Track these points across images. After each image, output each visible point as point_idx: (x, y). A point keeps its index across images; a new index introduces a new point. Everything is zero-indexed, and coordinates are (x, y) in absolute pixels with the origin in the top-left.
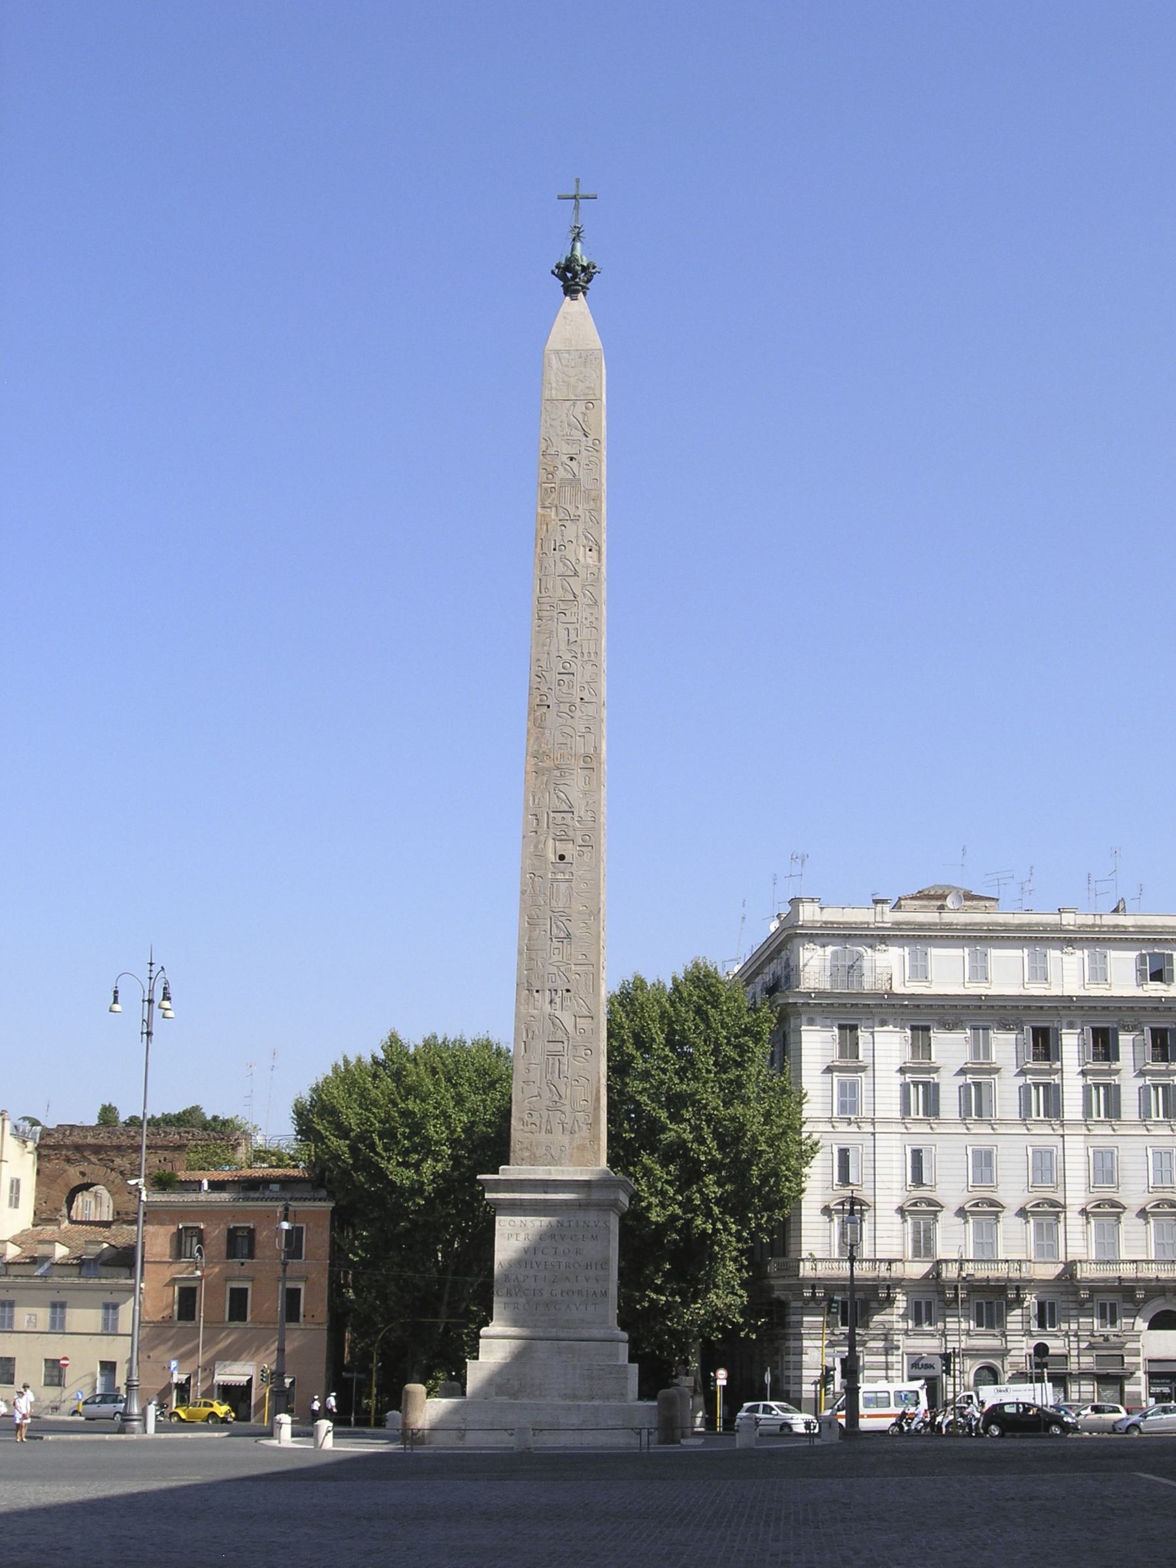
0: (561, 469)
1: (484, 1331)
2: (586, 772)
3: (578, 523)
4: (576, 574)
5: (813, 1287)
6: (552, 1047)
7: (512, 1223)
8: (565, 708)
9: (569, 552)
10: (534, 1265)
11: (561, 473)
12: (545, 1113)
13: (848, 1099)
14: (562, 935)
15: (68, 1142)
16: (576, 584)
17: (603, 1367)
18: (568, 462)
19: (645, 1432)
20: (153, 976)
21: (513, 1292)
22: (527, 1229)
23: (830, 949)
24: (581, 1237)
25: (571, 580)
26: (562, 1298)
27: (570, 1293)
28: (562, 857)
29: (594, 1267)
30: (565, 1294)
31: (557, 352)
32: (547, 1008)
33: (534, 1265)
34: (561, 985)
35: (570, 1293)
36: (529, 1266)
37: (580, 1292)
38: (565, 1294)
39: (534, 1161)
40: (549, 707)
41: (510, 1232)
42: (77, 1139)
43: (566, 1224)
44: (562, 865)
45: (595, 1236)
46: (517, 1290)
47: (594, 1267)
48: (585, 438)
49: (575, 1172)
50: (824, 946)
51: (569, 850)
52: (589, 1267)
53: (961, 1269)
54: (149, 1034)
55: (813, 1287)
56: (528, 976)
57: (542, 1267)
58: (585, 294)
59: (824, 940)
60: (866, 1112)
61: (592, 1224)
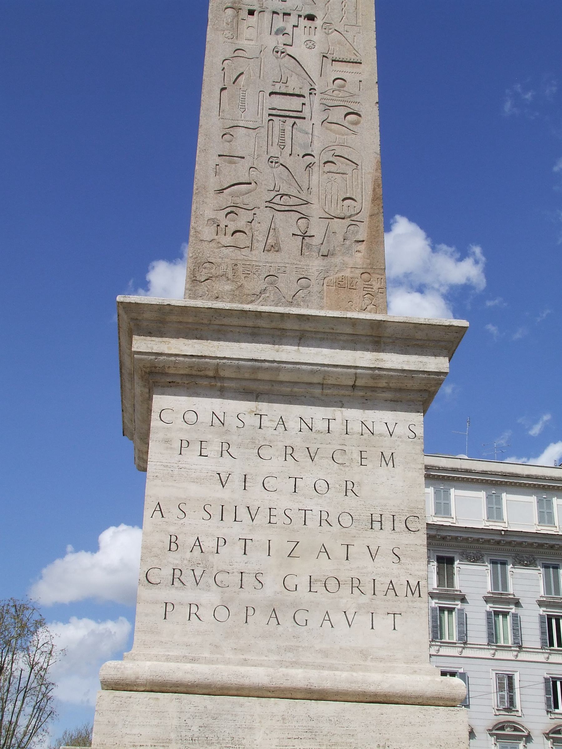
6: (280, 102)
7: (191, 417)
10: (243, 513)
12: (265, 215)
21: (188, 578)
22: (227, 432)
29: (388, 525)
33: (243, 513)
36: (229, 517)
43: (321, 425)
45: (387, 455)
47: (388, 525)
52: (377, 525)
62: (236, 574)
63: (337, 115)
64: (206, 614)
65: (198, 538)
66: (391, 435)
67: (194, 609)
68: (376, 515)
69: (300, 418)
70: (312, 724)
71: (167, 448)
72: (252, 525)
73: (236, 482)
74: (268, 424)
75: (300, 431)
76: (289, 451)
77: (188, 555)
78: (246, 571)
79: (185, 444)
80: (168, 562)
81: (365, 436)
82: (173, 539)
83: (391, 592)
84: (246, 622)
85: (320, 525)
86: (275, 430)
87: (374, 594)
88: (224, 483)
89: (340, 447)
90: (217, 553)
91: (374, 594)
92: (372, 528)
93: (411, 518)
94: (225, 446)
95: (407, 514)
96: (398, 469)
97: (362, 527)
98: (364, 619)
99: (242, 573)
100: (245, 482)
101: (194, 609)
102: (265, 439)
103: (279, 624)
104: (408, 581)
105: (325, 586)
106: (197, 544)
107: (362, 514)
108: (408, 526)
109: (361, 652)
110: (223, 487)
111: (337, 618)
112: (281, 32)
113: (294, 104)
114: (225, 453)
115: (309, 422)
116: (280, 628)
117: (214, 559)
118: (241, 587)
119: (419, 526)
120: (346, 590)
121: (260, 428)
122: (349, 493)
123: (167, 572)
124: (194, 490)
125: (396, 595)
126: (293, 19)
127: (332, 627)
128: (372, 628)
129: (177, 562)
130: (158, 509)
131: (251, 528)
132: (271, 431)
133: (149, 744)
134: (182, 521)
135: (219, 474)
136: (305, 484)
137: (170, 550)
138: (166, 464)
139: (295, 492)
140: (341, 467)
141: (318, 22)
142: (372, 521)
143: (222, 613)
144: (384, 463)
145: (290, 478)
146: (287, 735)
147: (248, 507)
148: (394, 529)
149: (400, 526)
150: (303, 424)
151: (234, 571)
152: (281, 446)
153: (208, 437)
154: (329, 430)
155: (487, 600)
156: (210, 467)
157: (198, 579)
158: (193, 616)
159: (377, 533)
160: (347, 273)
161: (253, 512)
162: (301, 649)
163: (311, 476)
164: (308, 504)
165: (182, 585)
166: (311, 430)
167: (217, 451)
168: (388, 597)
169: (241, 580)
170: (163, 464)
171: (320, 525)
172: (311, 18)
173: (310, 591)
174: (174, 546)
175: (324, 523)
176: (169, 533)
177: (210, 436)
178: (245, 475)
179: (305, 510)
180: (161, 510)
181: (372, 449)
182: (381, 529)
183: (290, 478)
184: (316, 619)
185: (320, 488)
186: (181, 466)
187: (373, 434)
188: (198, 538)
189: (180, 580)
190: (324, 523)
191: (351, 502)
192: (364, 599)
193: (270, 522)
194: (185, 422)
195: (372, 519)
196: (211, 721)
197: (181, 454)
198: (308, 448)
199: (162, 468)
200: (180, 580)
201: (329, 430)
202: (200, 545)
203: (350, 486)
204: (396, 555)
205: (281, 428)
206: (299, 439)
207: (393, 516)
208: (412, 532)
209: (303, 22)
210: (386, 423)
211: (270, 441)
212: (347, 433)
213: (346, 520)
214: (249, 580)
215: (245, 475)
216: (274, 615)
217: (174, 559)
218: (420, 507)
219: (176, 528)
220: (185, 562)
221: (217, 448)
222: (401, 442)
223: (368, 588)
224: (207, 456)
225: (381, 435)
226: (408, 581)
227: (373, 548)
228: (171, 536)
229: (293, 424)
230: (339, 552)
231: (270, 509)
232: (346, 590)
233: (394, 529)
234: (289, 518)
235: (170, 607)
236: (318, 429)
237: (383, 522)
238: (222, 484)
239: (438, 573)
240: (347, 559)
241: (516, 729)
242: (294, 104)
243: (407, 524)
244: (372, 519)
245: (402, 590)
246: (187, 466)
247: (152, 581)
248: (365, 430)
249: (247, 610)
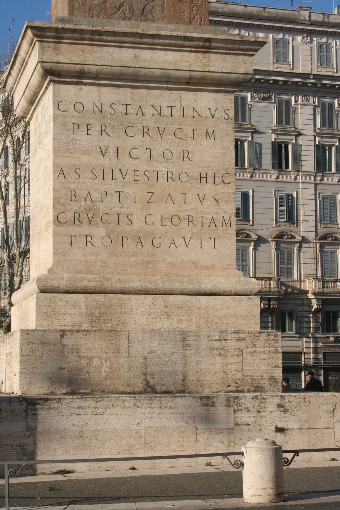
17: (243, 336)
24: (190, 132)
26: (163, 228)
27: (176, 220)
29: (211, 180)
30: (167, 222)
35: (176, 220)
36: (108, 177)
37: (190, 220)
38: (167, 222)
41: (76, 121)
43: (166, 112)
45: (211, 131)
46: (90, 215)
47: (211, 180)
49: (178, 30)
52: (203, 180)
57: (129, 177)
61: (206, 113)
62: (114, 215)
64: (97, 241)
65: (89, 192)
66: (213, 118)
67: (89, 239)
68: (203, 173)
69: (153, 106)
70: (166, 309)
71: (65, 130)
72: (124, 182)
73: (112, 152)
74: (132, 111)
75: (153, 116)
76: (146, 130)
77: (83, 204)
78: (121, 213)
79: (76, 127)
80: (70, 208)
81: (196, 118)
82: (73, 193)
83: (213, 224)
84: (122, 246)
85: (168, 181)
86: (136, 115)
87: (202, 226)
88: (104, 154)
89: (179, 127)
90: (102, 201)
91: (202, 226)
92: (200, 182)
93: (226, 175)
94: (103, 127)
95: (223, 172)
96: (218, 141)
97: (194, 182)
98: (195, 242)
99: (118, 214)
100: (118, 152)
101: (89, 239)
102: (130, 122)
103: (143, 247)
104: (223, 217)
105: (171, 221)
106: (89, 196)
107: (194, 173)
108: (223, 180)
109: (194, 263)
110: (104, 156)
111: (179, 242)
114: (104, 133)
115: (158, 108)
116: (144, 250)
117: (102, 207)
118: (118, 224)
119: (231, 180)
120: (184, 224)
121: (126, 114)
122: (186, 158)
123: (70, 215)
124: (85, 159)
125: (216, 226)
127: (176, 248)
128: (201, 248)
129: (76, 208)
130: (61, 172)
131: (123, 184)
132: (133, 116)
133: (70, 325)
134: (77, 181)
135: (100, 147)
136: (157, 153)
137: (71, 200)
138: (65, 141)
139: (151, 159)
140: (181, 141)
142: (200, 177)
143: (107, 241)
144: (208, 137)
145: (147, 149)
146: (152, 316)
147: (120, 170)
148: (214, 183)
149: (218, 180)
150: (155, 111)
151: (113, 213)
152: (140, 126)
153: (92, 121)
154: (172, 115)
156: (94, 143)
157: (90, 219)
158: (89, 243)
159: (204, 185)
161: (124, 173)
162: (157, 262)
163: (161, 147)
164: (159, 167)
165: (81, 223)
166: (160, 115)
167: (99, 131)
168: (211, 227)
169: (118, 219)
170: (63, 141)
171: (168, 181)
173: (162, 225)
174: (73, 198)
175: (170, 179)
176: (70, 189)
177: (93, 121)
178: (118, 148)
179: (158, 171)
180: (63, 174)
181: (201, 127)
182: (207, 183)
183: (147, 149)
184: (166, 243)
185: (166, 156)
186: (74, 142)
187: (201, 117)
188: (89, 192)
189: (79, 220)
190: (170, 179)
191: (187, 165)
192: (195, 229)
193: (135, 180)
194: (76, 110)
195: (200, 176)
196: (106, 310)
197: (74, 134)
198: (158, 128)
199: (62, 144)
200: (79, 220)
201: (172, 115)
202: (90, 197)
203: (186, 154)
204: (216, 200)
205: (140, 114)
206: (152, 122)
207: (214, 173)
208: (226, 185)
210: (210, 109)
211: (133, 123)
212: (184, 117)
213: (184, 178)
214: (123, 219)
215: (118, 148)
216: (139, 241)
217: (74, 206)
218: (231, 167)
219: (75, 185)
220: (82, 208)
221: (98, 129)
222: (220, 122)
223: (198, 222)
224: (92, 135)
225: (206, 117)
226: (223, 217)
227: (201, 196)
228: (71, 191)
229: (148, 111)
230: (179, 198)
231: (135, 171)
232: (184, 224)
233: (214, 183)
234: (148, 177)
235: (74, 239)
236: (165, 114)
237: (207, 178)
238: (103, 154)
240: (185, 204)
243: (223, 179)
244: (200, 176)
245: (219, 223)
246: (78, 142)
247: (61, 221)
248: (196, 114)
249: (123, 238)
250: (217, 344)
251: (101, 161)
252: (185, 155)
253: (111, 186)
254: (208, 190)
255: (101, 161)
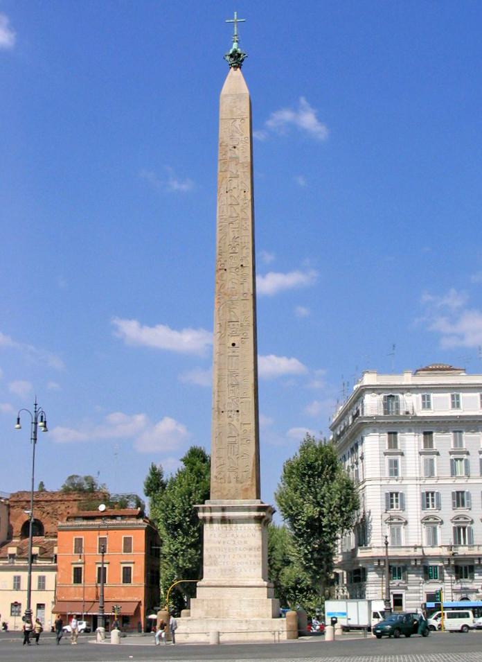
0: (229, 152)
1: (199, 583)
2: (245, 301)
3: (239, 179)
4: (238, 204)
5: (379, 561)
8: (233, 270)
9: (235, 193)
11: (229, 155)
13: (393, 468)
14: (234, 383)
15: (22, 499)
16: (238, 208)
18: (233, 149)
19: (277, 633)
20: (37, 410)
23: (382, 396)
25: (236, 207)
28: (234, 345)
31: (226, 96)
32: (228, 420)
34: (233, 407)
39: (223, 497)
40: (225, 270)
42: (26, 498)
44: (234, 349)
48: (240, 137)
50: (379, 394)
51: (236, 340)
53: (451, 550)
54: (35, 439)
55: (379, 561)
56: (218, 405)
57: (227, 551)
58: (240, 68)
59: (380, 391)
60: (400, 474)
63: (245, 441)
111: (243, 570)
112: (230, 417)
113: (234, 439)
126: (233, 412)
136: (236, 542)
141: (240, 412)
155: (451, 453)
160: (247, 487)
172: (238, 411)
209: (236, 413)
239: (424, 441)
241: (465, 518)
242: (234, 439)
250: (251, 603)
251: (218, 545)
252: (245, 542)
253: (221, 553)
254: (253, 553)
255: (218, 545)
